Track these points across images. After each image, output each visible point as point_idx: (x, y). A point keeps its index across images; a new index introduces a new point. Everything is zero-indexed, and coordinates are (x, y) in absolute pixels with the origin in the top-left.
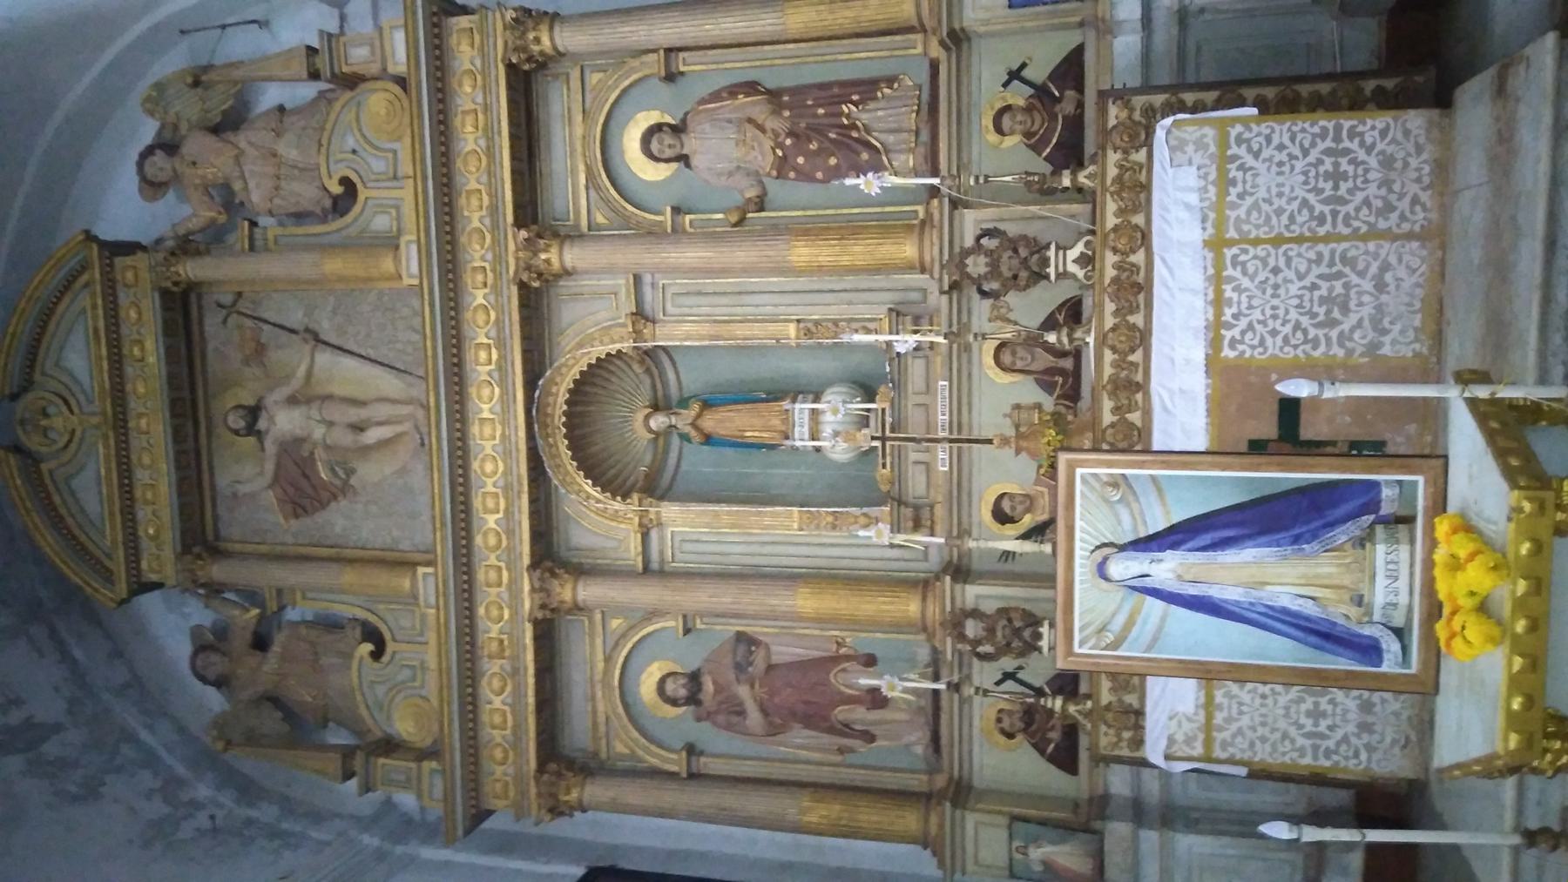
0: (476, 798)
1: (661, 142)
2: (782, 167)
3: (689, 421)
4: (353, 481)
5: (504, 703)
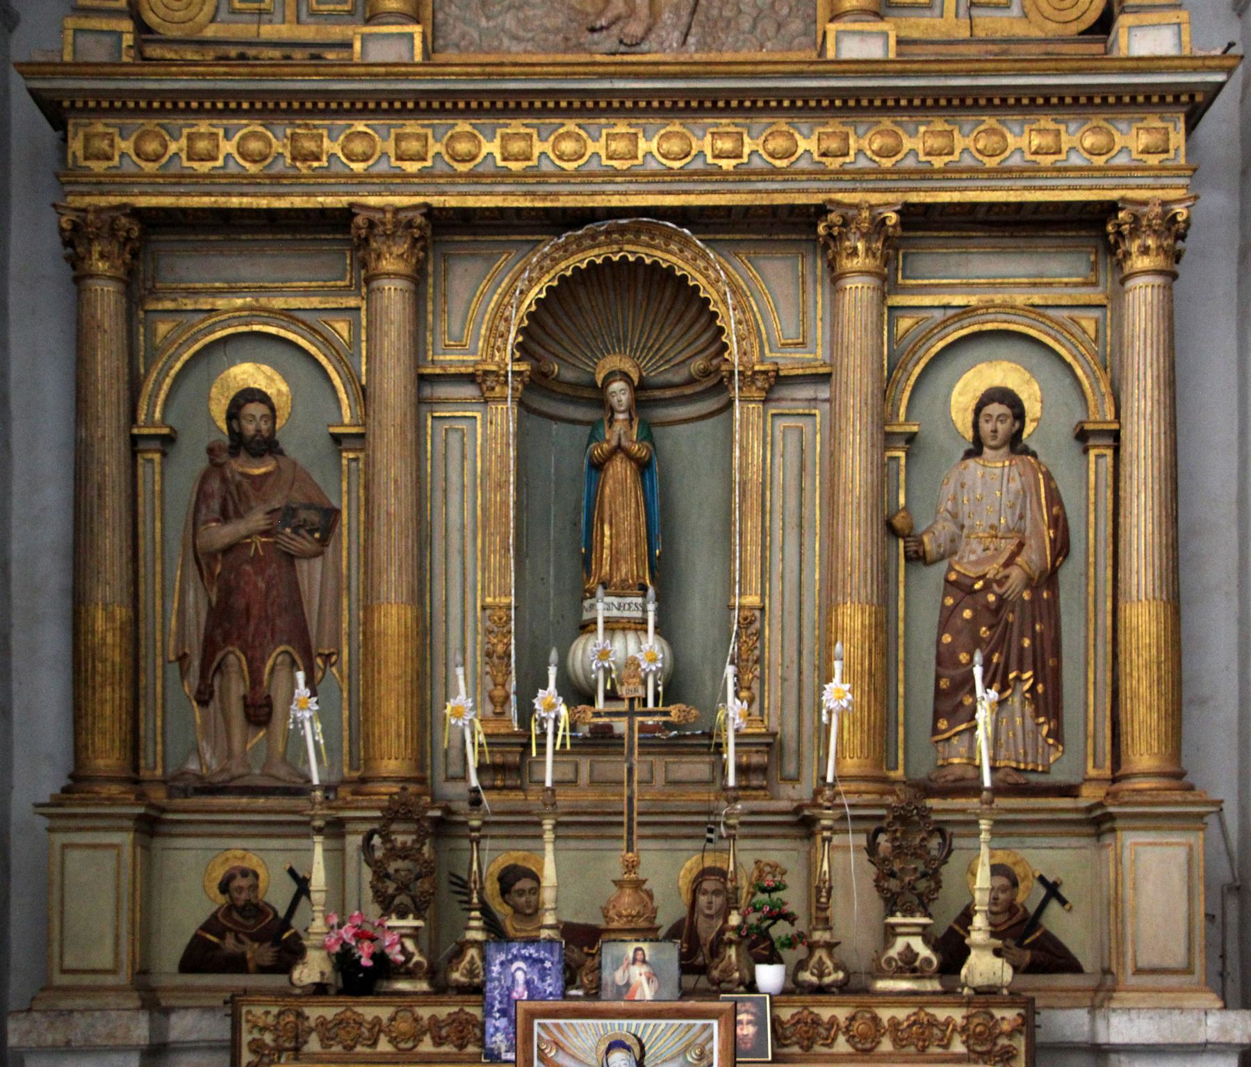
0: (85, 110)
1: (1001, 418)
2: (961, 588)
3: (625, 443)
5: (228, 156)
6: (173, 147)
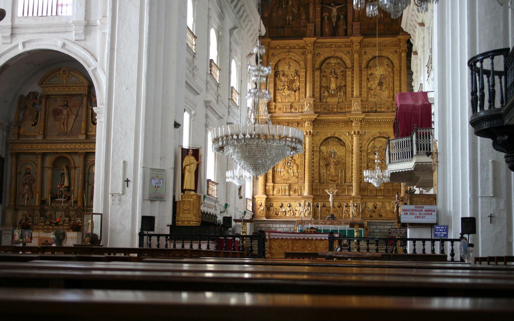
4: (57, 122)
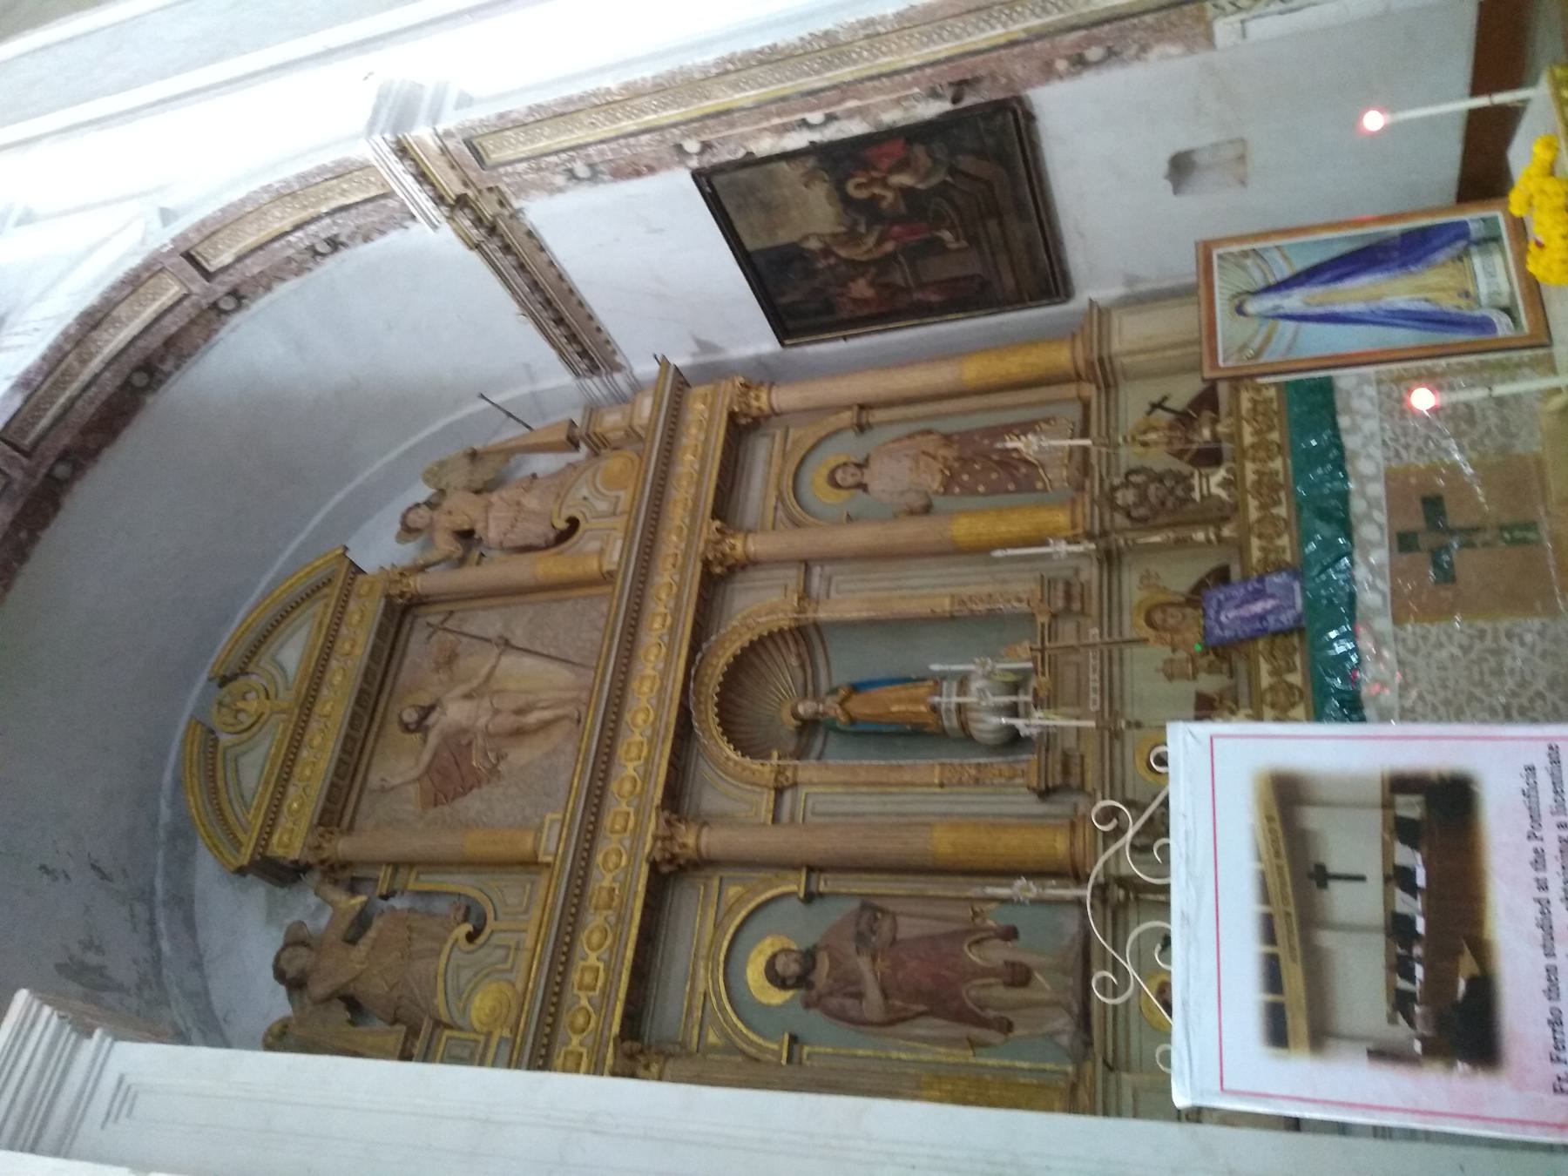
4: (502, 767)
5: (598, 959)
6: (584, 1002)
